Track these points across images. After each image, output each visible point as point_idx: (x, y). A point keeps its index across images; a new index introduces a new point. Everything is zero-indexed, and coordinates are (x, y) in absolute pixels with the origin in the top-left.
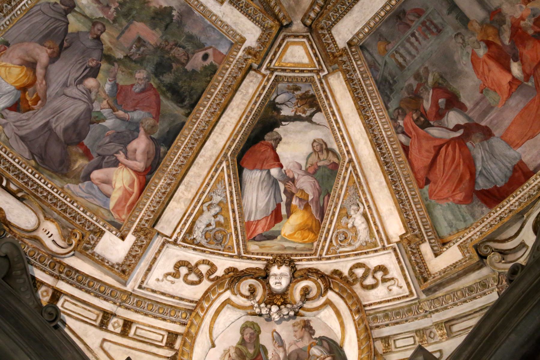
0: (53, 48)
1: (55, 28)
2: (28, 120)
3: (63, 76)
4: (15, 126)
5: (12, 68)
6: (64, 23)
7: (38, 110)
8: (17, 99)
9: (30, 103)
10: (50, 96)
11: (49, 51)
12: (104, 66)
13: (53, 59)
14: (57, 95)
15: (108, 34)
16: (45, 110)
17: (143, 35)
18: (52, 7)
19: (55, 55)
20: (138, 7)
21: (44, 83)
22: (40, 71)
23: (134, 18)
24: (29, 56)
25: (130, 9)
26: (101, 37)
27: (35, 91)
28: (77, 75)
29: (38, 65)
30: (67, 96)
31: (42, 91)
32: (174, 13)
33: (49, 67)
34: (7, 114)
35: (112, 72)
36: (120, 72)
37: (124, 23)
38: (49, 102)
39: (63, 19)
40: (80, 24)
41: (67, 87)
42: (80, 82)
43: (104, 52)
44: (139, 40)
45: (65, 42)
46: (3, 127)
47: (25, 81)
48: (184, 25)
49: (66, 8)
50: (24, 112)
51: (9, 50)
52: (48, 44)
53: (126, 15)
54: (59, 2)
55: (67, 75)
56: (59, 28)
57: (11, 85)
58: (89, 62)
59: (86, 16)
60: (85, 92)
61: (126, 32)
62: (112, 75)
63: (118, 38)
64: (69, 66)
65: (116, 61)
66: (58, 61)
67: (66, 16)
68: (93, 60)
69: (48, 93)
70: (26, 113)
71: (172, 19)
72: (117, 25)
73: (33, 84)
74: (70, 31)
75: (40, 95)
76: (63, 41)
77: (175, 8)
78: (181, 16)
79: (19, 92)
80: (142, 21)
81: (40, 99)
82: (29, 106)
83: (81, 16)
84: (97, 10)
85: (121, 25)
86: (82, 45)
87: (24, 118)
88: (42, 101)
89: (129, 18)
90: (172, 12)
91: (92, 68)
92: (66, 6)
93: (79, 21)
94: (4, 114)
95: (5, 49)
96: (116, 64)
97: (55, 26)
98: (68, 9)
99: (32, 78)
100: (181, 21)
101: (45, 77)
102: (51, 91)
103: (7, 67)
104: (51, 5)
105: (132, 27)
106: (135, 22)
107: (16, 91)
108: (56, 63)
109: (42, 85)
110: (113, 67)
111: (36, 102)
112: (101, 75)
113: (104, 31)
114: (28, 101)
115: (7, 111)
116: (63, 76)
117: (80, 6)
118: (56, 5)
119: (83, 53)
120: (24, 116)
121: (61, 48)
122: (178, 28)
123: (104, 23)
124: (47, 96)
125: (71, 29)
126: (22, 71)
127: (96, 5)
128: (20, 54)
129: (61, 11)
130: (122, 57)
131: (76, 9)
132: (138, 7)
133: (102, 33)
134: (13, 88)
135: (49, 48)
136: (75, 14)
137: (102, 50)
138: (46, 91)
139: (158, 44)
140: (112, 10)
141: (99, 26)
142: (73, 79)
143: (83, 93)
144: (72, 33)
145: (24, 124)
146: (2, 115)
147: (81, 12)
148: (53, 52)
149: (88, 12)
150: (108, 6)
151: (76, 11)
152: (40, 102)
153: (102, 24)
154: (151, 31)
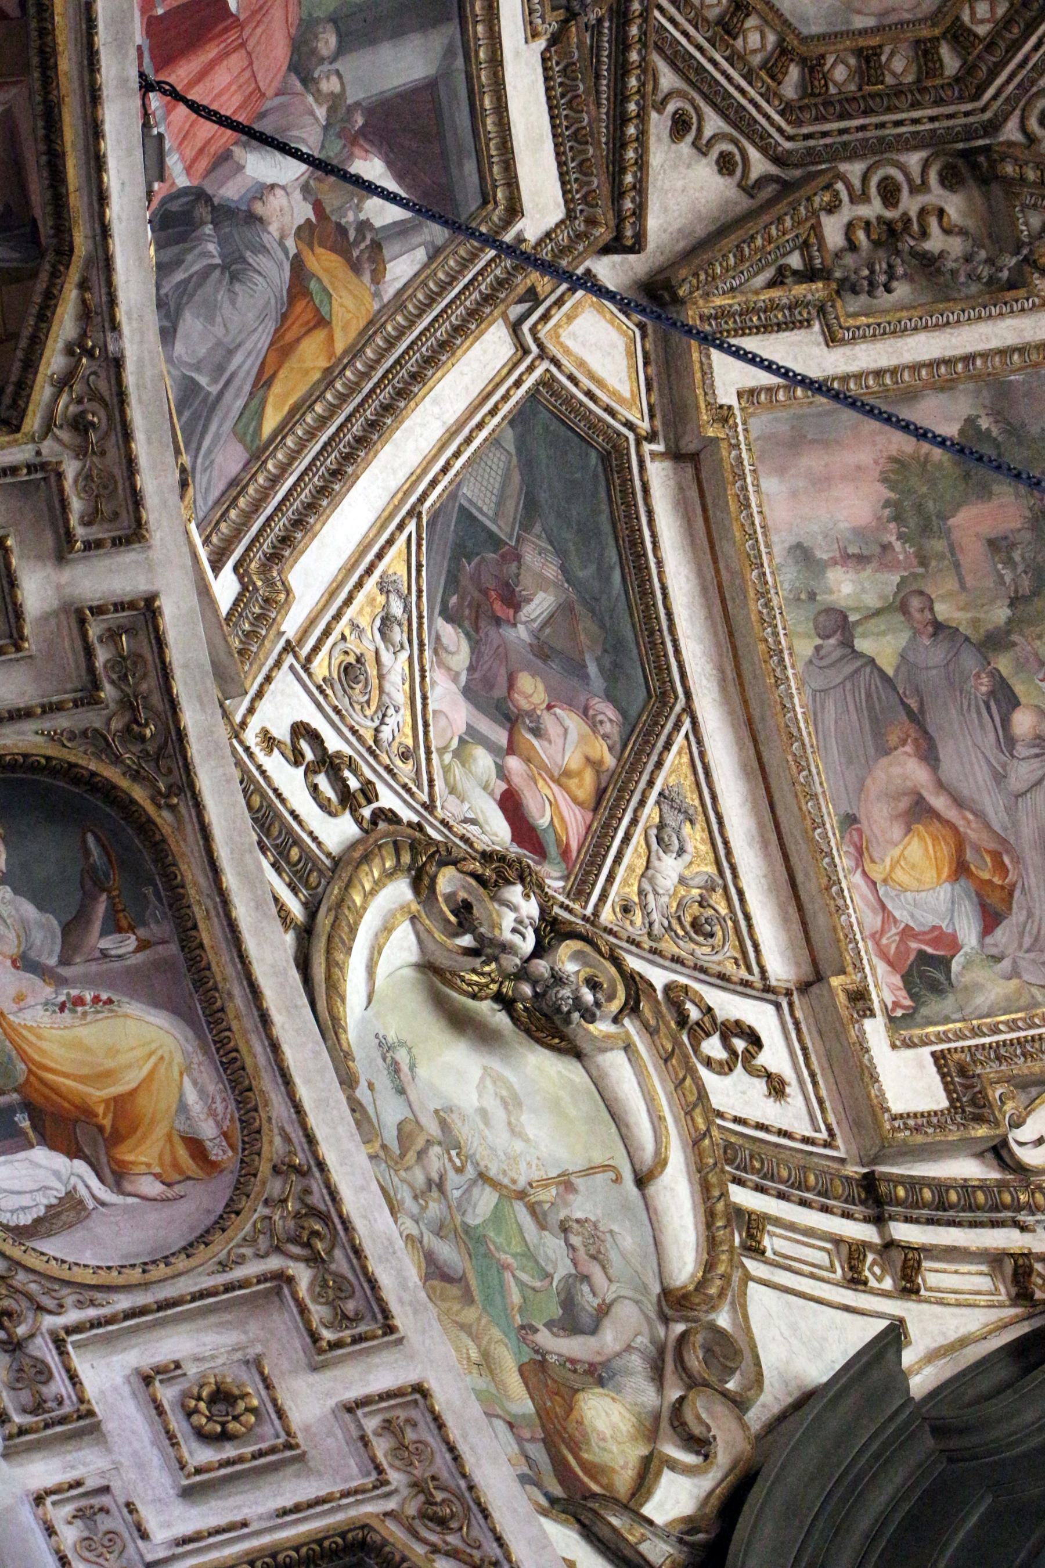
0: (908, 736)
1: (869, 695)
2: (1030, 915)
3: (977, 767)
4: (1028, 951)
5: (906, 853)
6: (868, 670)
7: (1020, 876)
8: (975, 899)
9: (997, 880)
10: (1006, 829)
11: (908, 748)
12: (1003, 664)
13: (929, 755)
14: (1011, 810)
15: (942, 598)
16: (1029, 862)
17: (989, 528)
18: (823, 663)
19: (924, 745)
20: (924, 489)
21: (971, 817)
22: (939, 803)
23: (943, 517)
24: (897, 797)
25: (919, 508)
26: (940, 618)
27: (977, 849)
28: (992, 736)
29: (925, 794)
30: (1025, 793)
31: (985, 836)
32: (984, 423)
33: (943, 779)
34: (996, 945)
35: (1027, 659)
36: (1038, 643)
37: (938, 545)
38: (1017, 839)
39: (859, 663)
40: (889, 637)
41: (1005, 777)
42: (1008, 741)
43: (974, 638)
44: (993, 544)
45: (908, 701)
46: (1019, 977)
47: (946, 851)
48: (1023, 425)
49: (838, 636)
50: (1010, 909)
51: (864, 826)
52: (893, 739)
53: (926, 529)
54: (818, 641)
55: (980, 756)
56: (873, 687)
57: (939, 884)
58: (977, 689)
59: (878, 613)
60: (1037, 751)
61: (960, 557)
62: (1033, 665)
63: (963, 586)
64: (964, 736)
65: (1008, 633)
66: (940, 750)
67: (854, 651)
68: (978, 676)
69: (997, 828)
70: (1014, 906)
71: (995, 439)
72: (933, 563)
73: (960, 843)
74: (890, 672)
75: (992, 845)
76: (903, 703)
77: (974, 413)
78: (999, 413)
79: (963, 881)
80: (958, 506)
81: (1000, 854)
82: (1002, 887)
83: (873, 621)
84: (878, 575)
85: (941, 557)
86: (934, 672)
87: (1022, 918)
88: (1007, 852)
89: (935, 529)
90: (978, 429)
91: (992, 693)
92: (835, 632)
93: (883, 634)
94: (994, 951)
95: (860, 831)
96: (1015, 637)
97: (863, 691)
98: (843, 634)
99: (947, 832)
100: (1009, 424)
101: (959, 802)
102: (997, 818)
103: (898, 862)
104: (816, 662)
105: (956, 535)
106: (951, 522)
107: (957, 886)
108: (941, 756)
109: (974, 825)
110: (1017, 648)
111: (1001, 868)
112: (1019, 689)
113: (931, 601)
114: (990, 882)
115: (989, 940)
116: (977, 767)
117: (851, 603)
118: (822, 652)
119: (952, 684)
120: (1017, 916)
121: (917, 718)
122: (1020, 443)
123: (915, 587)
124: (1000, 831)
125: (888, 664)
126: (922, 839)
127: (869, 571)
128: (885, 813)
129: (838, 653)
130: (1008, 612)
131: (852, 618)
132: (924, 489)
133: (931, 609)
134: (947, 886)
135: (904, 743)
136: (860, 630)
137: (967, 639)
138: (988, 826)
139: (1028, 514)
140: (898, 545)
141: (915, 603)
142: (995, 751)
143: (1037, 756)
144: (897, 670)
145: (1035, 931)
146: (993, 957)
147: (865, 613)
148: (916, 740)
149: (872, 601)
150: (886, 547)
151: (858, 623)
152: (1006, 860)
153: (914, 592)
154: (991, 505)
